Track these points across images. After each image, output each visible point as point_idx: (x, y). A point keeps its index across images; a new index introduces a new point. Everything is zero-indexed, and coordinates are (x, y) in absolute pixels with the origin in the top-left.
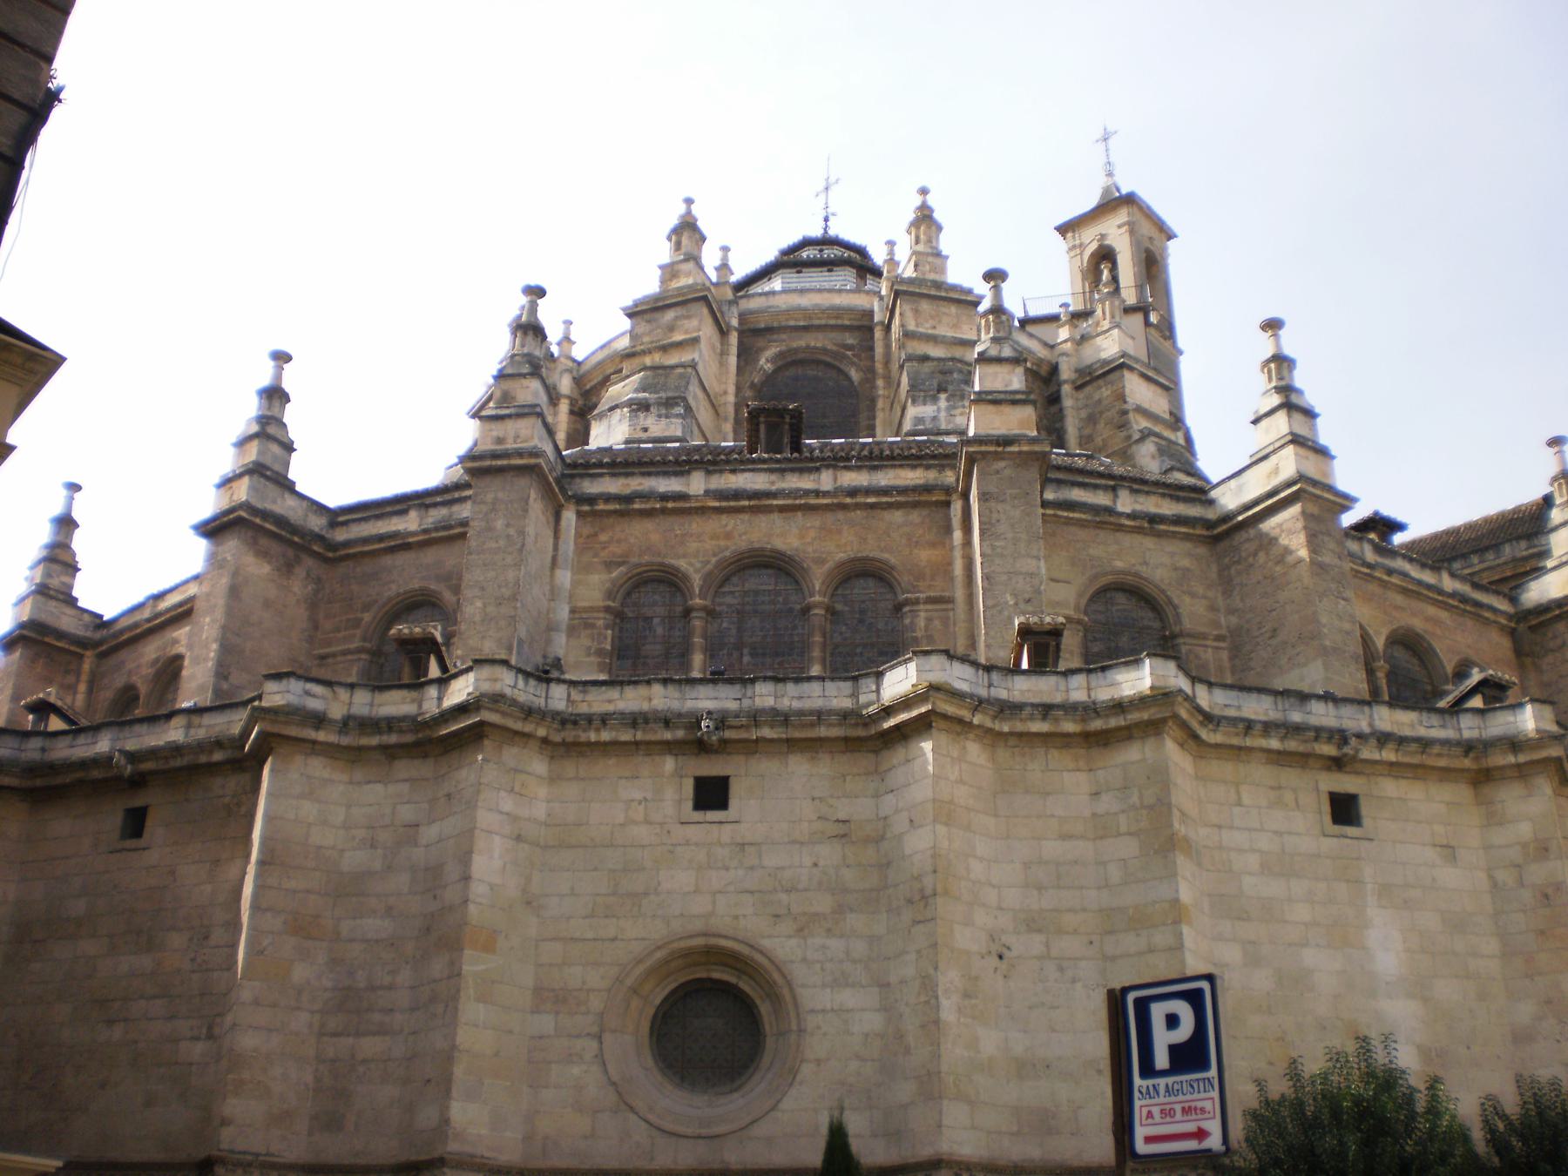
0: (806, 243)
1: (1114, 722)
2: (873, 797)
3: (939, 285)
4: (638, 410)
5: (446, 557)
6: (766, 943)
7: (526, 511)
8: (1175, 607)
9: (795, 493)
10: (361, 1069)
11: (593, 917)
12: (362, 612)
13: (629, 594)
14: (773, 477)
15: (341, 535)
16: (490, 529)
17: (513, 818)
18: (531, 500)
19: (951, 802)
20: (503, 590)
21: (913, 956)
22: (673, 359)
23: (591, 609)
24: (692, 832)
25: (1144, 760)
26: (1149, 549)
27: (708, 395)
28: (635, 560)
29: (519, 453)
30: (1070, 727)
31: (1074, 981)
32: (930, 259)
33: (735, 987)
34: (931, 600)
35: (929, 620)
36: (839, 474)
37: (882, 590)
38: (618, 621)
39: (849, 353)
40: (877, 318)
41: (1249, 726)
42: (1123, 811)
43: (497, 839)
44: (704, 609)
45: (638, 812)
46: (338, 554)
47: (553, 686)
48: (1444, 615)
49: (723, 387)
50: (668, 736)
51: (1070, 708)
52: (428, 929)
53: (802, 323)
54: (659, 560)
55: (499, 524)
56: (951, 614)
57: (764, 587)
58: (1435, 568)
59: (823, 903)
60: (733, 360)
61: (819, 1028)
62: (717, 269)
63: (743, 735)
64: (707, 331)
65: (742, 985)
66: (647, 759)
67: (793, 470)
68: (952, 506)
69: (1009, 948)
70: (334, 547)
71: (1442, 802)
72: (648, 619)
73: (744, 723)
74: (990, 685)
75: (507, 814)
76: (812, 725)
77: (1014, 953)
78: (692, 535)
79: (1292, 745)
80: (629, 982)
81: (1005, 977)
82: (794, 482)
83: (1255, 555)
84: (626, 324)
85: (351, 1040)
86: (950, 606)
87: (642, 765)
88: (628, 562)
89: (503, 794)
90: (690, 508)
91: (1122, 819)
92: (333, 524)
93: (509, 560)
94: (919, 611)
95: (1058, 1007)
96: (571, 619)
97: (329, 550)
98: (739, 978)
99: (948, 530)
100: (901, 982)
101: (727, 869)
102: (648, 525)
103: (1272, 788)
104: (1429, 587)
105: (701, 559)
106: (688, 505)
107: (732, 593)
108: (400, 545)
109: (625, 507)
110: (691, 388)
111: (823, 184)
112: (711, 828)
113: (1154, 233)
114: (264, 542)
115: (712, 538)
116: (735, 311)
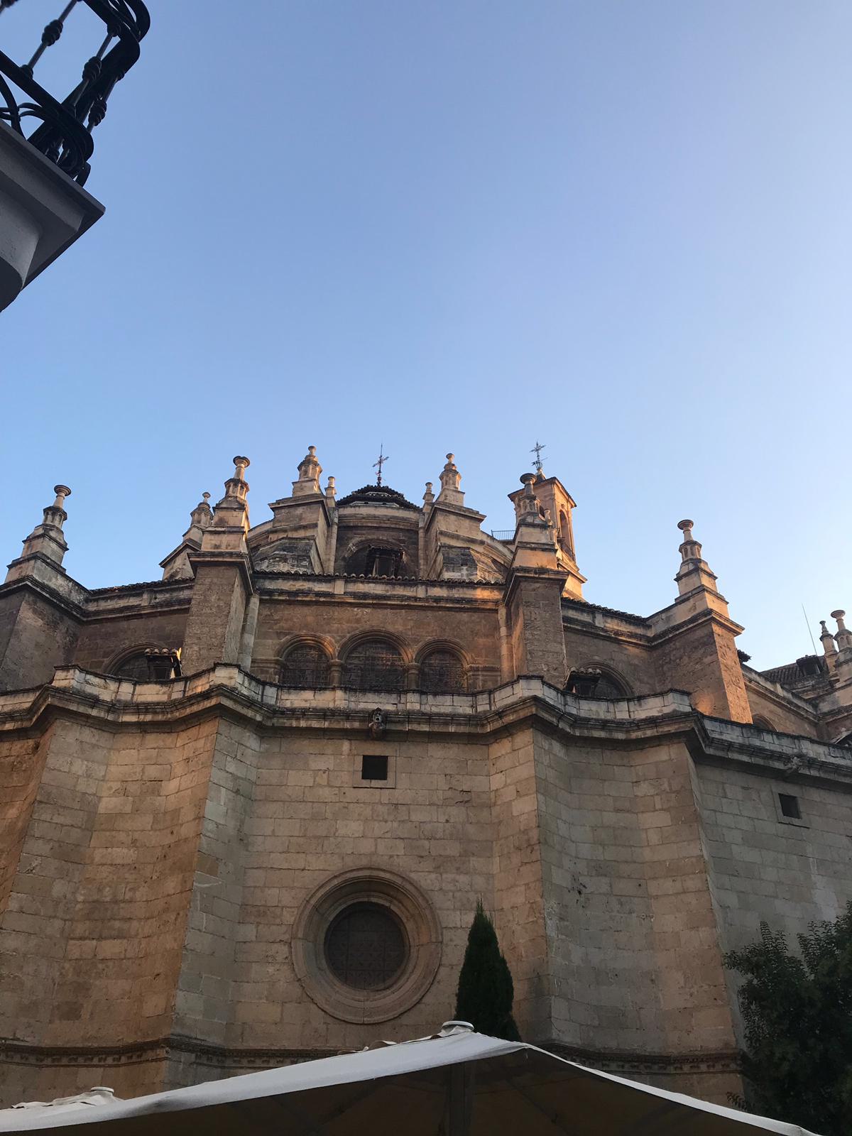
0: (369, 488)
1: (649, 733)
2: (487, 776)
3: (461, 508)
4: (279, 561)
5: (169, 625)
6: (413, 875)
7: (233, 591)
8: (631, 688)
9: (402, 598)
10: (100, 966)
11: (289, 852)
12: (103, 657)
13: (290, 654)
14: (388, 587)
15: (92, 607)
16: (206, 601)
17: (235, 778)
18: (236, 585)
19: (545, 780)
20: (213, 640)
21: (523, 888)
22: (301, 534)
23: (267, 661)
24: (362, 794)
25: (671, 760)
26: (614, 651)
27: (320, 560)
28: (297, 632)
29: (231, 554)
30: (621, 736)
31: (630, 913)
32: (454, 493)
33: (388, 909)
34: (485, 669)
35: (485, 681)
36: (428, 588)
37: (455, 662)
38: (283, 670)
39: (402, 545)
40: (421, 525)
41: (730, 746)
42: (657, 794)
43: (223, 790)
44: (341, 665)
45: (322, 779)
46: (90, 619)
47: (267, 687)
48: (779, 710)
49: (328, 557)
50: (347, 725)
51: (620, 725)
52: (165, 856)
53: (375, 525)
54: (313, 633)
55: (213, 598)
56: (499, 678)
57: (380, 656)
58: (773, 682)
59: (453, 849)
60: (334, 541)
61: (451, 940)
62: (326, 489)
63: (399, 727)
64: (321, 522)
65: (392, 907)
66: (330, 742)
67: (400, 585)
68: (499, 612)
69: (584, 886)
70: (86, 614)
71: (847, 807)
72: (303, 672)
73: (400, 719)
74: (566, 704)
75: (231, 773)
76: (446, 724)
77: (588, 891)
78: (334, 619)
79: (754, 760)
80: (313, 902)
81: (583, 907)
82: (400, 591)
83: (681, 658)
84: (270, 515)
85: (94, 942)
86: (499, 673)
87: (329, 746)
88: (292, 633)
89: (229, 759)
90: (335, 602)
91: (657, 799)
92: (87, 601)
93: (219, 621)
94: (479, 675)
95: (621, 931)
96: (251, 667)
97: (84, 617)
98: (391, 902)
99: (497, 628)
100: (512, 908)
101: (386, 822)
102: (306, 610)
103: (743, 788)
104: (771, 692)
105: (340, 634)
106: (333, 600)
107: (359, 657)
108: (133, 614)
109: (293, 599)
110: (312, 552)
111: (379, 459)
112: (373, 793)
113: (564, 502)
114: (40, 605)
115: (347, 623)
116: (336, 513)
